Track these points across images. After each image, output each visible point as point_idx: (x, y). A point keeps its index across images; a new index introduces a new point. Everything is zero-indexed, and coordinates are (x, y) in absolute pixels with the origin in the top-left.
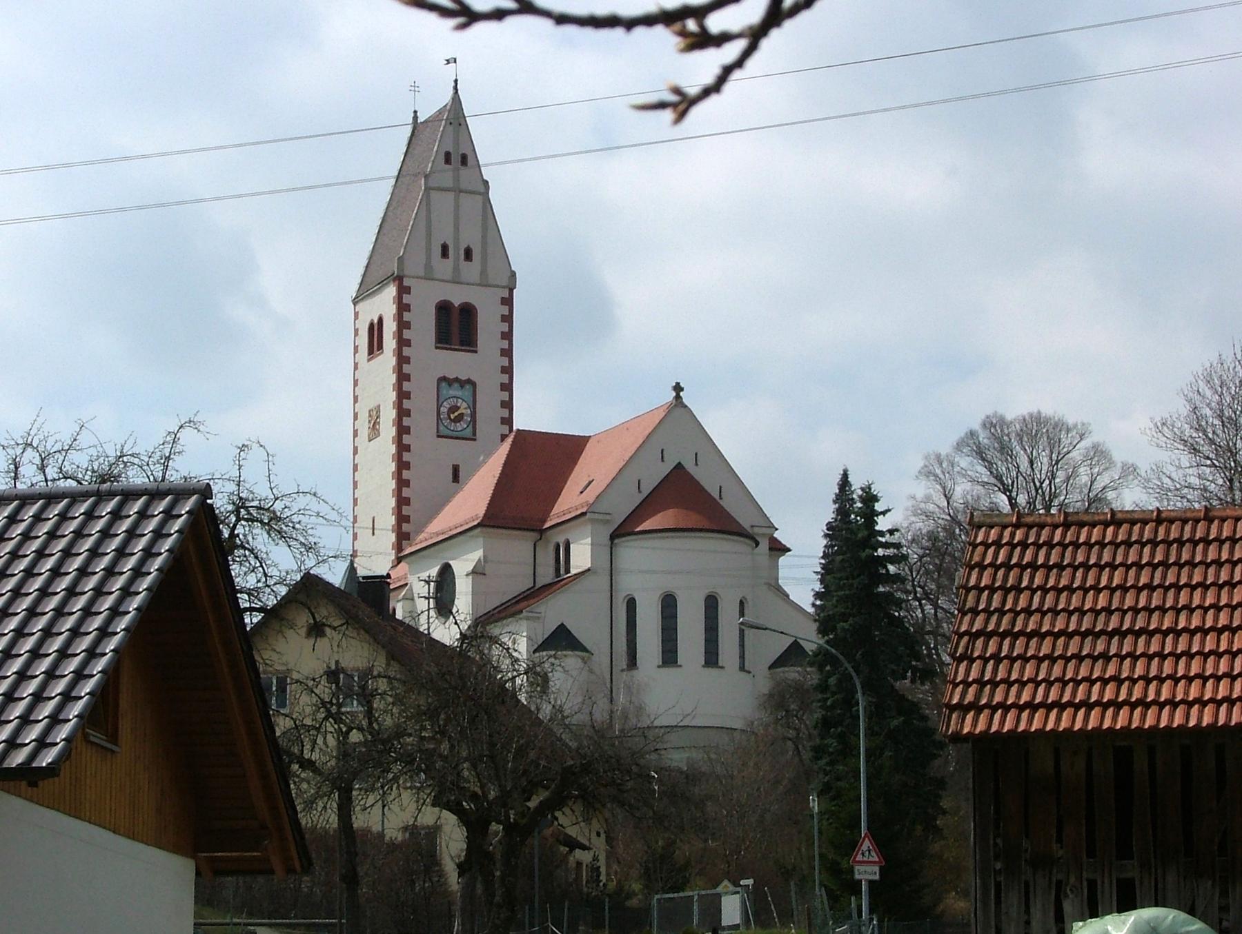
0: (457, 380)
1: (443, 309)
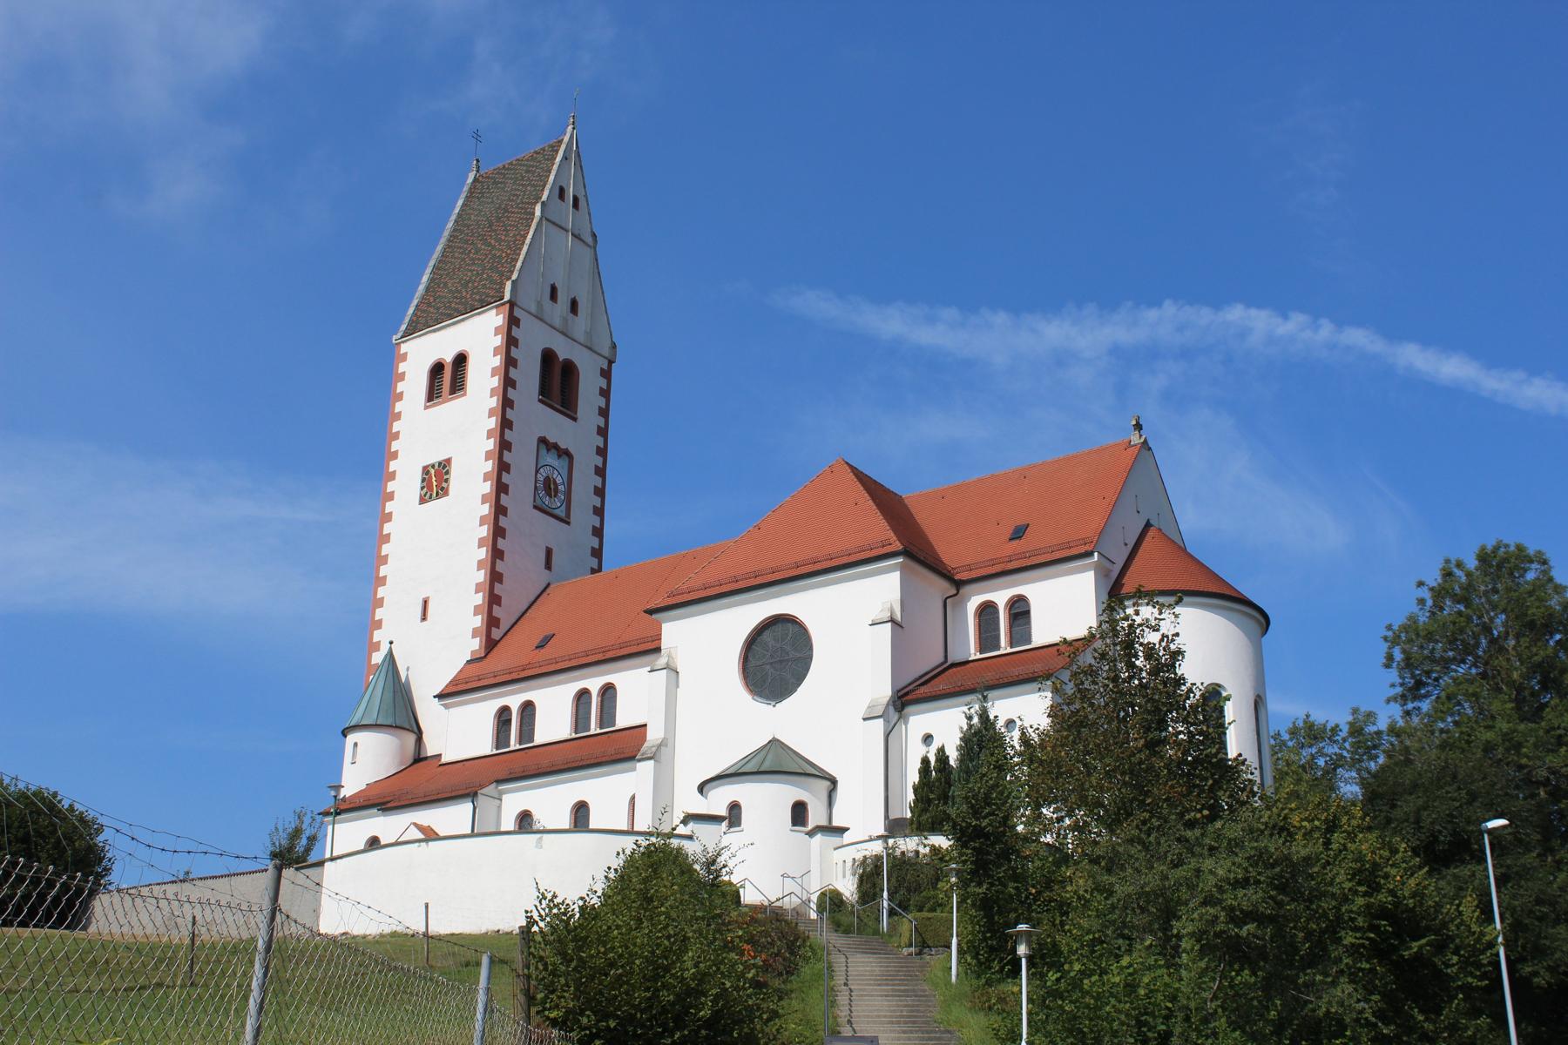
0: (555, 446)
1: (548, 357)
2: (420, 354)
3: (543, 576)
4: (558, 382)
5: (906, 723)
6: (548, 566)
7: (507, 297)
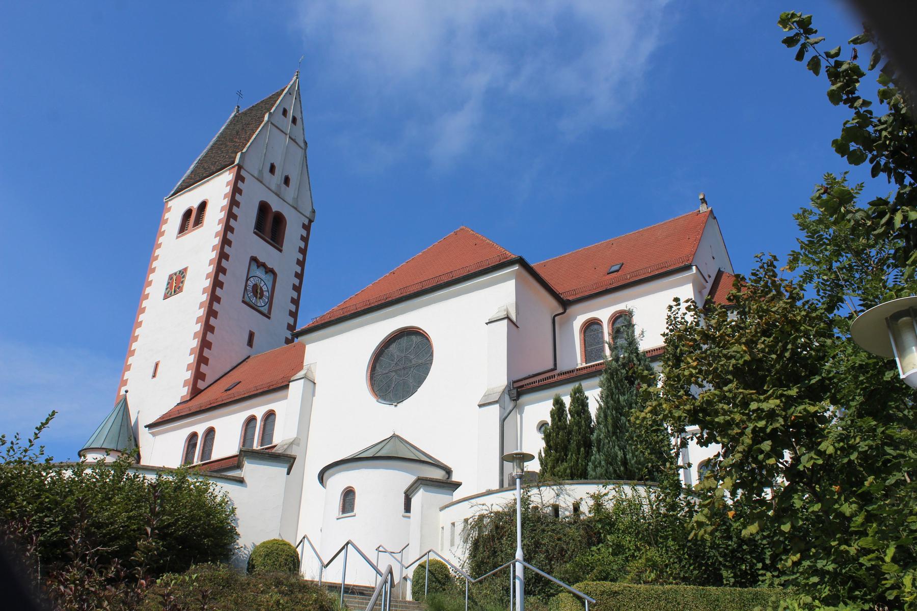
0: (263, 265)
1: (264, 208)
2: (178, 206)
3: (247, 351)
4: (270, 225)
5: (521, 413)
6: (250, 343)
7: (237, 162)
